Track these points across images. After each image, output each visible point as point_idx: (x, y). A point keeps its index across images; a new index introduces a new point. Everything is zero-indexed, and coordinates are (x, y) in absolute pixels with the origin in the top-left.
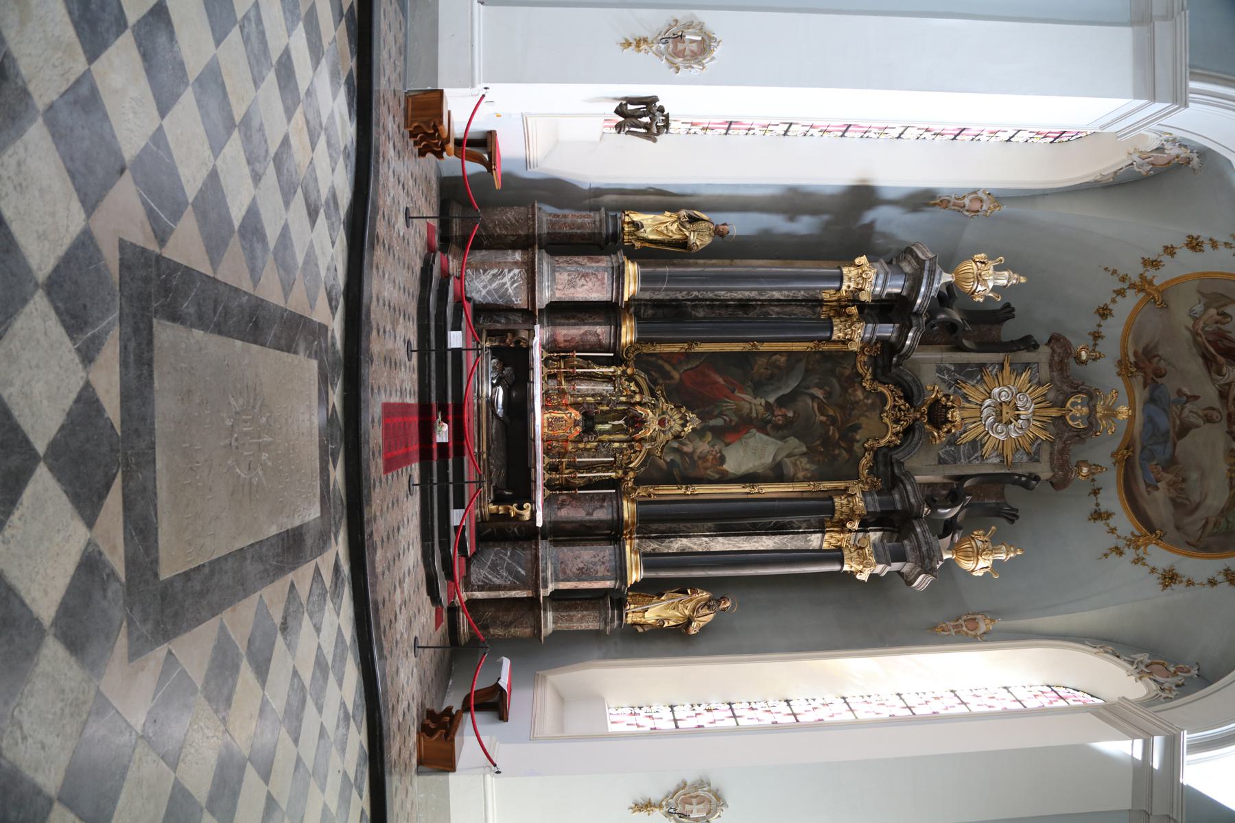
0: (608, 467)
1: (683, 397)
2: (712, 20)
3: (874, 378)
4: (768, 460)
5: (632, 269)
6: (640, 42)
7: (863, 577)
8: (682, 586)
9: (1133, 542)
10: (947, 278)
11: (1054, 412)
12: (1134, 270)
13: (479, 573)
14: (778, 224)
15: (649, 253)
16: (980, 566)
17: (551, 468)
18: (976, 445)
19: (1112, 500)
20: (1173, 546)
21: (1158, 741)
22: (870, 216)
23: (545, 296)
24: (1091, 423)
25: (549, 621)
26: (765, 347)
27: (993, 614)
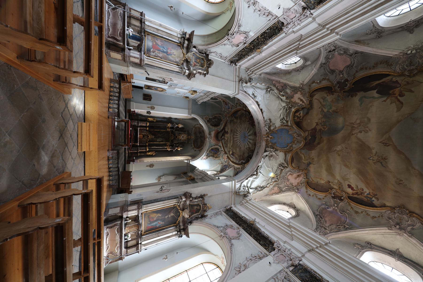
0: (145, 140)
1: (152, 134)
2: (155, 106)
3: (171, 134)
4: (161, 140)
5: (148, 123)
6: (149, 107)
7: (169, 150)
8: (152, 151)
9: (194, 148)
10: (177, 126)
11: (187, 137)
12: (194, 126)
13: (132, 149)
14: (163, 120)
15: (150, 122)
16: (179, 149)
17: (139, 140)
18: (181, 140)
19: (193, 145)
20: (195, 148)
21: (188, 161)
22: (171, 120)
23: (139, 125)
24: (190, 138)
25: (139, 154)
26: (161, 130)
27: (181, 154)
